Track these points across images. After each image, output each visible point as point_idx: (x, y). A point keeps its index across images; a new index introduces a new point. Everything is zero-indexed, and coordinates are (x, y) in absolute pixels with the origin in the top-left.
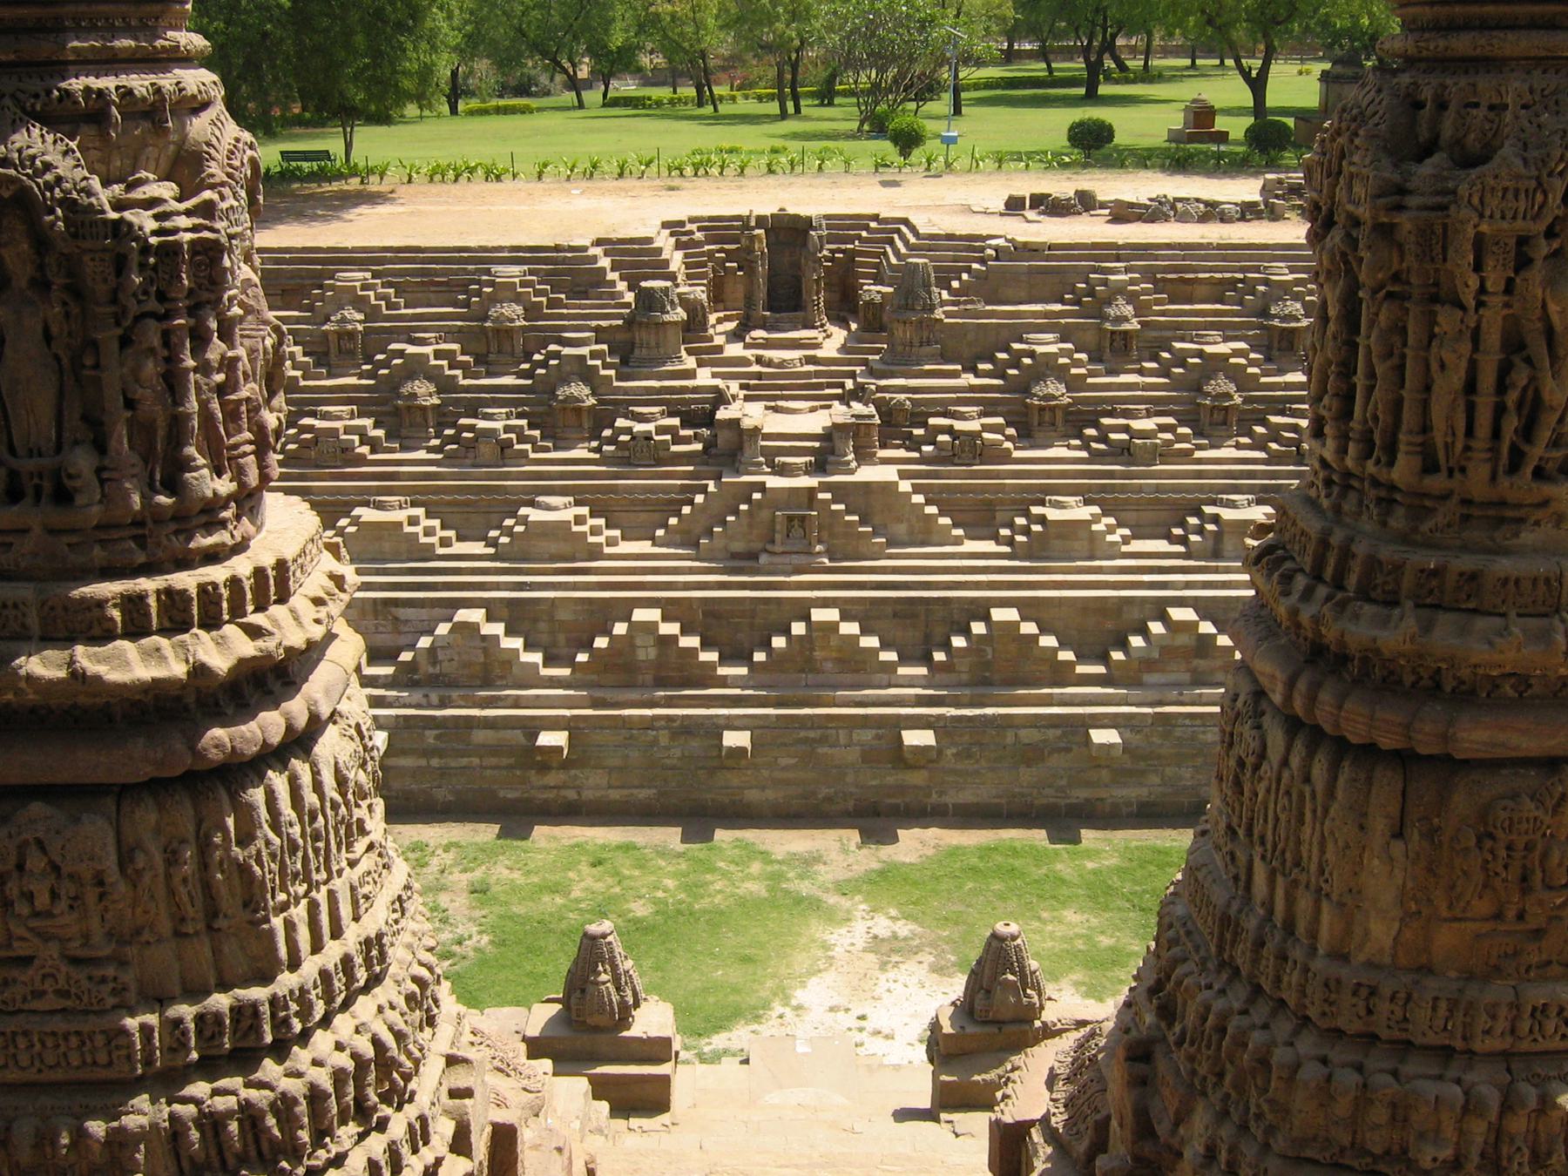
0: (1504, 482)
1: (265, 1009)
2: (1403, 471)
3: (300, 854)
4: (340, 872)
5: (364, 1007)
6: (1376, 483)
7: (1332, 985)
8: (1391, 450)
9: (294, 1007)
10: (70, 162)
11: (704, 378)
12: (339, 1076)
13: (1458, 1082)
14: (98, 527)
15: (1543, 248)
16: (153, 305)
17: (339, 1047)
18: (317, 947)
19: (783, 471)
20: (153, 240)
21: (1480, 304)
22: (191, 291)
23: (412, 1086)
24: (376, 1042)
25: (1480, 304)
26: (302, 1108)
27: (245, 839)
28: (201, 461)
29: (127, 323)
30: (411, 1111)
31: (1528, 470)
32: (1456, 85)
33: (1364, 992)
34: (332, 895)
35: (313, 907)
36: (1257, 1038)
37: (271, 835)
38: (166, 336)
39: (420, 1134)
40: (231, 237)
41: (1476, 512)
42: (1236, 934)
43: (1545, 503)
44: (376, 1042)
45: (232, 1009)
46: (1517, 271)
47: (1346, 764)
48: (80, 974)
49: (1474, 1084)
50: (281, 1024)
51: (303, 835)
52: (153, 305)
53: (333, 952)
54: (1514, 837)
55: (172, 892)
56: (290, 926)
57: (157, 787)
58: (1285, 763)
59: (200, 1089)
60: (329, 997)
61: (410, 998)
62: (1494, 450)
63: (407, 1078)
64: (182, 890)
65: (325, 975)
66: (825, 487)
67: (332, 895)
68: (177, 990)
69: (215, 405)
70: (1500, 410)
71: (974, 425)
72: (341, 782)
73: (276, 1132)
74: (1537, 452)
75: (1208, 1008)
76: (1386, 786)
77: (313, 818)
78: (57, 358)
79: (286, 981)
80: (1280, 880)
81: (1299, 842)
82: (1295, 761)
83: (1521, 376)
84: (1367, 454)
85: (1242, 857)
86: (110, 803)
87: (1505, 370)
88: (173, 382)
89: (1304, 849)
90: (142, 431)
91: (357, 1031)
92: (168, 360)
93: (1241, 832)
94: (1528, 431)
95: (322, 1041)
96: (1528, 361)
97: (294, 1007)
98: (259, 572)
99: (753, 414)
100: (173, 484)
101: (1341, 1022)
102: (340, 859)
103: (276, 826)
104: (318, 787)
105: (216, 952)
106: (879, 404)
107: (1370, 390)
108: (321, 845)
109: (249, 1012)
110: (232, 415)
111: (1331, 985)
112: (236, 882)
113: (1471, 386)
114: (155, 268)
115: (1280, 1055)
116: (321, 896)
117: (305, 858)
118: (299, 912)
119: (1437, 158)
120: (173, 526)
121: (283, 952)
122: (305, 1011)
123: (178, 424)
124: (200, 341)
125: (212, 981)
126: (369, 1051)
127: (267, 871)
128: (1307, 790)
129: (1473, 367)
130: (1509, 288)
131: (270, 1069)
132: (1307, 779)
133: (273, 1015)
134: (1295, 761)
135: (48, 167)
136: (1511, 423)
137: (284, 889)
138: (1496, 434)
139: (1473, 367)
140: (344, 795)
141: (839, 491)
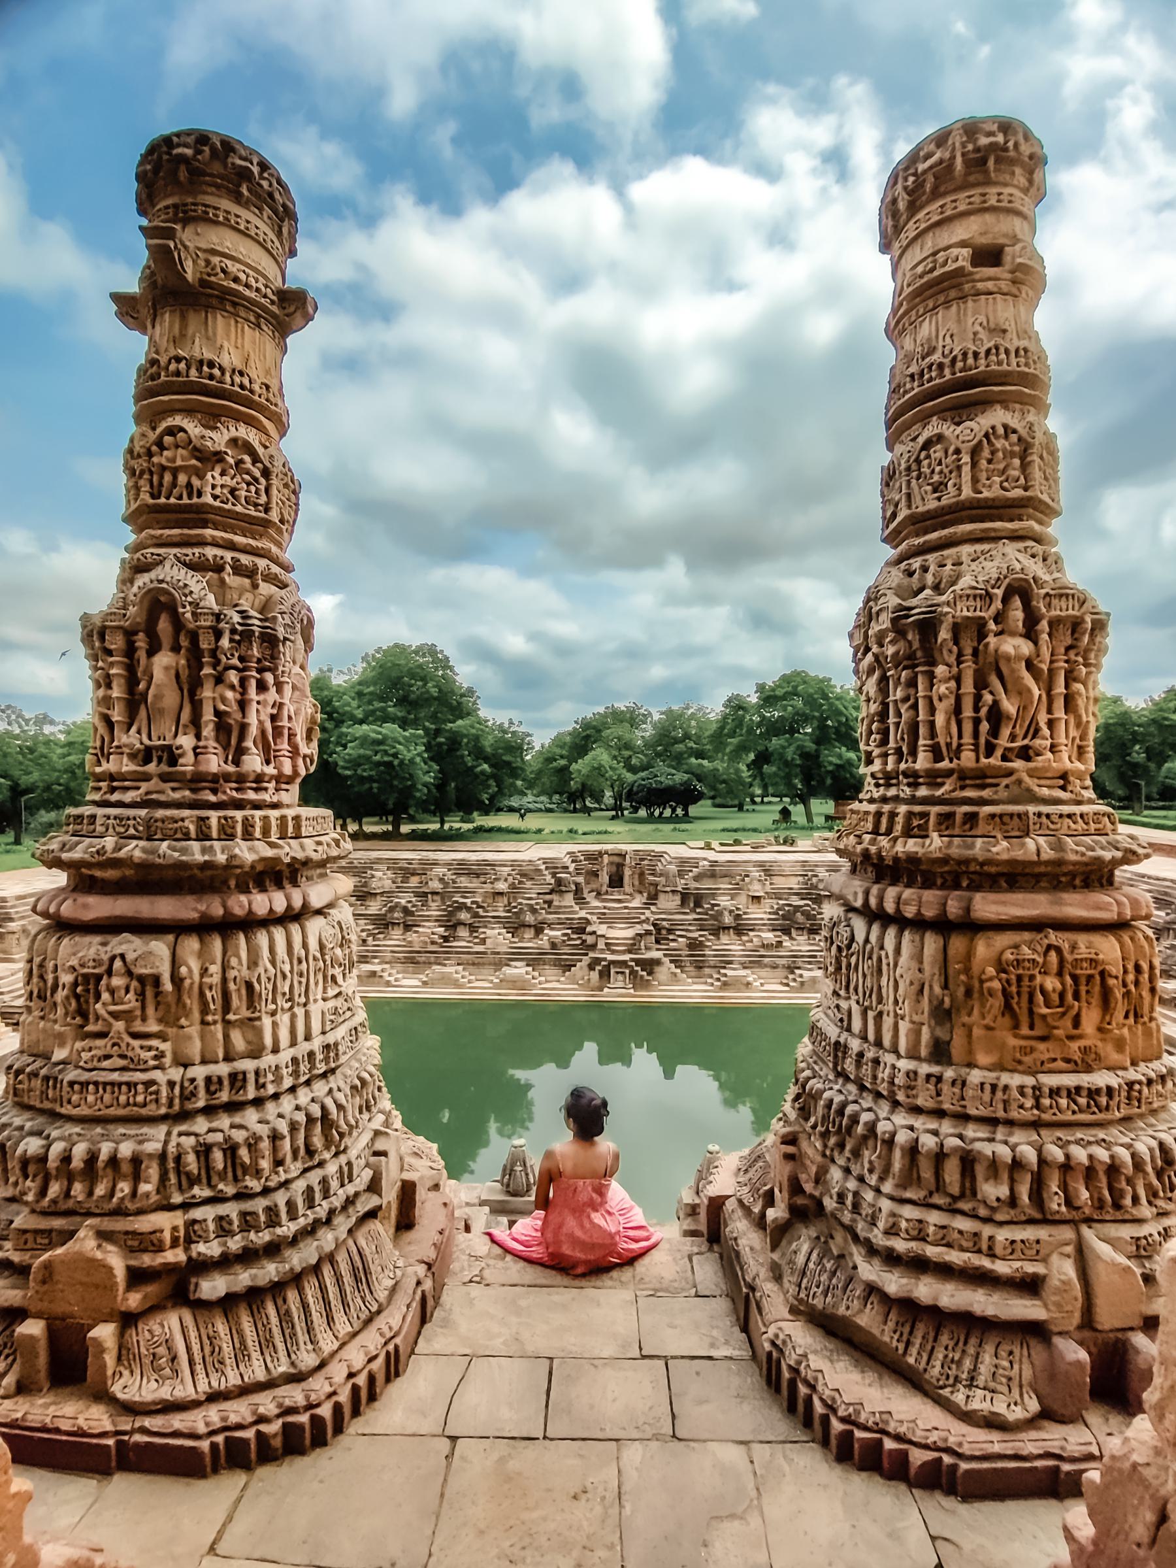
0: (984, 760)
1: (251, 1078)
2: (923, 762)
3: (288, 982)
4: (315, 1001)
5: (320, 1088)
6: (906, 774)
8: (913, 753)
9: (270, 1077)
10: (200, 586)
11: (583, 914)
12: (293, 1127)
13: (1006, 1143)
14: (191, 781)
15: (992, 626)
16: (235, 661)
17: (298, 1108)
18: (293, 1043)
19: (613, 952)
20: (239, 628)
21: (959, 663)
22: (259, 661)
23: (347, 1141)
24: (323, 1108)
25: (959, 663)
26: (265, 1145)
27: (253, 963)
28: (254, 750)
29: (220, 668)
30: (343, 1159)
31: (999, 753)
32: (932, 558)
33: (933, 1080)
34: (307, 1015)
35: (293, 1018)
36: (865, 1117)
37: (269, 966)
38: (243, 682)
39: (347, 1175)
40: (285, 639)
41: (968, 782)
42: (845, 1053)
43: (1010, 773)
44: (323, 1108)
45: (230, 1075)
46: (979, 642)
47: (906, 933)
48: (136, 1043)
49: (1016, 1145)
50: (260, 1086)
51: (291, 972)
52: (235, 661)
53: (303, 1048)
54: (1021, 971)
55: (202, 994)
56: (275, 1025)
57: (203, 928)
58: (867, 941)
59: (201, 1125)
60: (296, 1074)
61: (354, 1088)
62: (976, 745)
63: (342, 1135)
64: (209, 995)
65: (295, 1061)
66: (632, 960)
67: (307, 1015)
68: (197, 1060)
69: (268, 726)
70: (977, 722)
71: (695, 935)
72: (322, 947)
73: (247, 1160)
74: (1003, 741)
75: (831, 1101)
76: (932, 943)
77: (300, 962)
78: (181, 689)
79: (268, 1060)
80: (871, 1014)
81: (880, 988)
82: (873, 938)
83: (988, 698)
84: (899, 761)
85: (844, 1005)
86: (171, 938)
87: (978, 698)
88: (243, 705)
89: (884, 991)
90: (222, 726)
91: (313, 1100)
92: (242, 694)
93: (842, 993)
94: (995, 732)
95: (287, 1104)
96: (991, 693)
97: (270, 1077)
98: (283, 818)
99: (602, 929)
100: (237, 762)
101: (920, 1102)
102: (317, 992)
103: (273, 962)
104: (305, 945)
105: (226, 1037)
106: (654, 925)
107: (897, 724)
108: (304, 980)
109: (240, 1077)
110: (278, 732)
111: (912, 1075)
112: (244, 992)
113: (957, 710)
114: (239, 643)
115: (883, 1127)
116: (299, 1011)
117: (291, 987)
118: (284, 1019)
119: (928, 592)
120: (234, 785)
121: (268, 1041)
122: (278, 1080)
123: (243, 728)
124: (262, 687)
125: (221, 1056)
126: (316, 1111)
127: (263, 989)
128: (883, 953)
129: (958, 699)
130: (975, 653)
131: (250, 1117)
132: (882, 948)
133: (257, 1081)
134: (873, 938)
135: (186, 585)
136: (985, 726)
137: (274, 1001)
138: (976, 734)
139: (958, 699)
140: (323, 954)
141: (638, 962)
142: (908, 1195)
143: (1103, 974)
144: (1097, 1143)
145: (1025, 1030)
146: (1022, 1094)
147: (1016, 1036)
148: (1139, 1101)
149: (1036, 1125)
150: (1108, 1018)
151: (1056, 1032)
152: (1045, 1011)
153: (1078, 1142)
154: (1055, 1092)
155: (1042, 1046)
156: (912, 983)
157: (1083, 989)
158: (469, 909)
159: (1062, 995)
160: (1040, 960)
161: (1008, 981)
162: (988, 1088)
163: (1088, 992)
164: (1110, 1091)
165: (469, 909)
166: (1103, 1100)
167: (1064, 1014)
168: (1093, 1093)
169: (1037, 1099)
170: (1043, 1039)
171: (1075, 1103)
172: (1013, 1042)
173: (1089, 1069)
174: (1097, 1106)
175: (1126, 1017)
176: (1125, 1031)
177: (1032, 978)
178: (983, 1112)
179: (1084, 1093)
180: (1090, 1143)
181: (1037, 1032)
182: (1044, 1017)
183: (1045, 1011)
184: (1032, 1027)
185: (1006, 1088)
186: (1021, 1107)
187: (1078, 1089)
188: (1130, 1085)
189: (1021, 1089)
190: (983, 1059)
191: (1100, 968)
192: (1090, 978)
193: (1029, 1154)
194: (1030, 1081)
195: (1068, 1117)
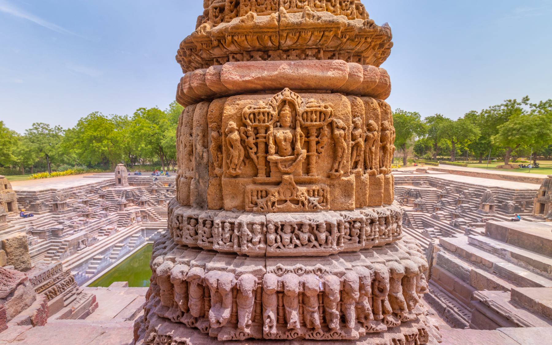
7: (180, 218)
13: (234, 271)
33: (193, 221)
49: (241, 273)
142: (167, 315)
143: (331, 125)
144: (314, 272)
145: (262, 177)
146: (252, 231)
147: (255, 183)
148: (359, 237)
149: (265, 257)
150: (336, 166)
151: (286, 177)
152: (275, 157)
153: (296, 271)
154: (280, 228)
155: (273, 189)
156: (186, 146)
157: (313, 139)
158: (157, 185)
159: (293, 144)
160: (275, 113)
161: (246, 133)
162: (227, 225)
163: (318, 143)
164: (329, 228)
165: (157, 185)
166: (323, 236)
167: (294, 160)
168: (315, 229)
169: (265, 234)
170: (278, 184)
171: (298, 238)
172: (250, 187)
173: (314, 209)
174: (316, 239)
175: (355, 166)
176: (352, 177)
177: (267, 129)
178: (226, 248)
179: (306, 229)
180: (307, 272)
181: (274, 178)
182: (276, 163)
183: (275, 157)
184: (268, 175)
185: (240, 225)
186: (250, 241)
187: (301, 226)
188: (352, 223)
189: (251, 225)
190: (228, 203)
191: (329, 120)
192: (320, 129)
193: (249, 282)
194: (259, 219)
195: (290, 250)
